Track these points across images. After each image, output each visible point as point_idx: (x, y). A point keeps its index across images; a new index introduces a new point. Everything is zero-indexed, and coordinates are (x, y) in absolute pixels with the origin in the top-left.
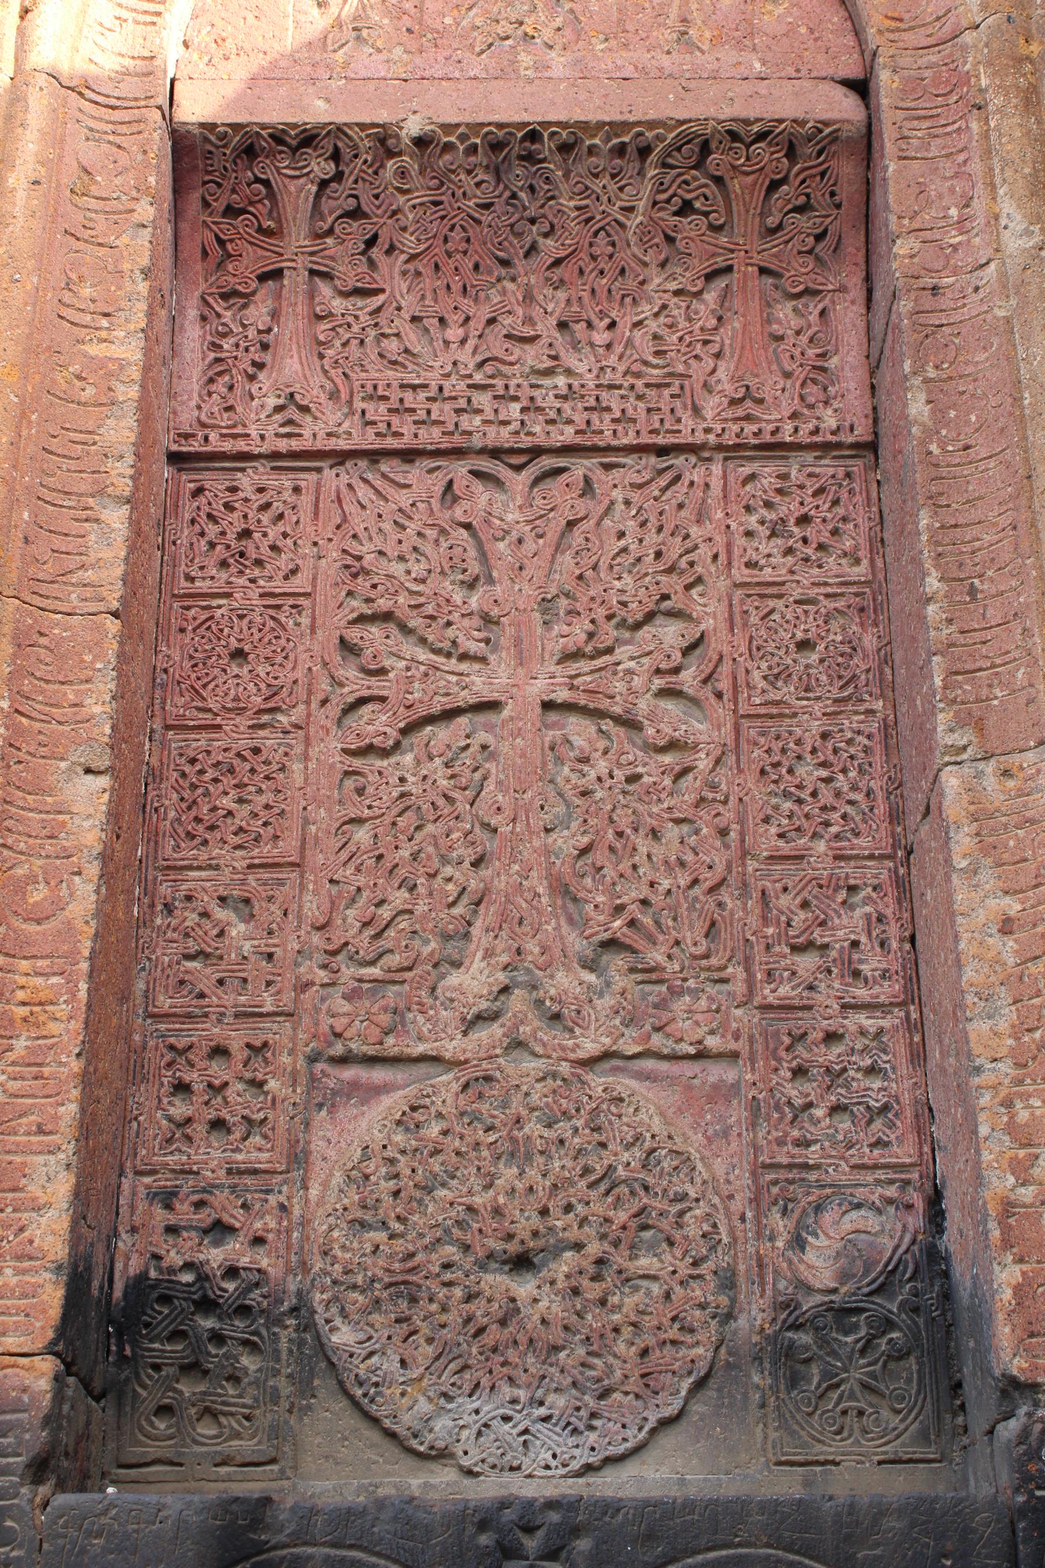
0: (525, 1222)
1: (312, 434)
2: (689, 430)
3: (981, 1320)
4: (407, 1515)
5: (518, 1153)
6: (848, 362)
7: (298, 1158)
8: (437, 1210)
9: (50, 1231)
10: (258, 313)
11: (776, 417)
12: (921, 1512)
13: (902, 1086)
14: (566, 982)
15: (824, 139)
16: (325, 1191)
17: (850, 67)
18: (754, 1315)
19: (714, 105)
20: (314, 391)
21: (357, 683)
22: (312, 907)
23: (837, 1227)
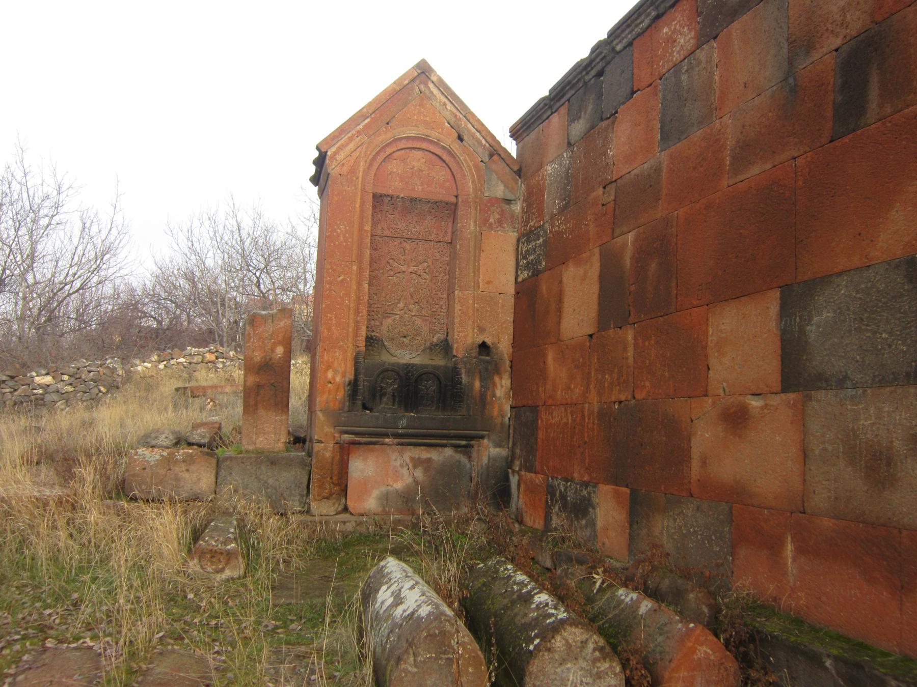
0: (405, 333)
1: (385, 233)
2: (430, 238)
3: (452, 348)
4: (398, 364)
5: (405, 325)
6: (449, 231)
7: (382, 324)
8: (396, 331)
9: (364, 334)
10: (379, 216)
11: (440, 238)
12: (446, 367)
13: (446, 321)
14: (411, 306)
15: (452, 204)
16: (384, 328)
17: (455, 194)
18: (428, 344)
19: (439, 198)
20: (385, 227)
21: (389, 268)
22: (384, 295)
23: (437, 336)
